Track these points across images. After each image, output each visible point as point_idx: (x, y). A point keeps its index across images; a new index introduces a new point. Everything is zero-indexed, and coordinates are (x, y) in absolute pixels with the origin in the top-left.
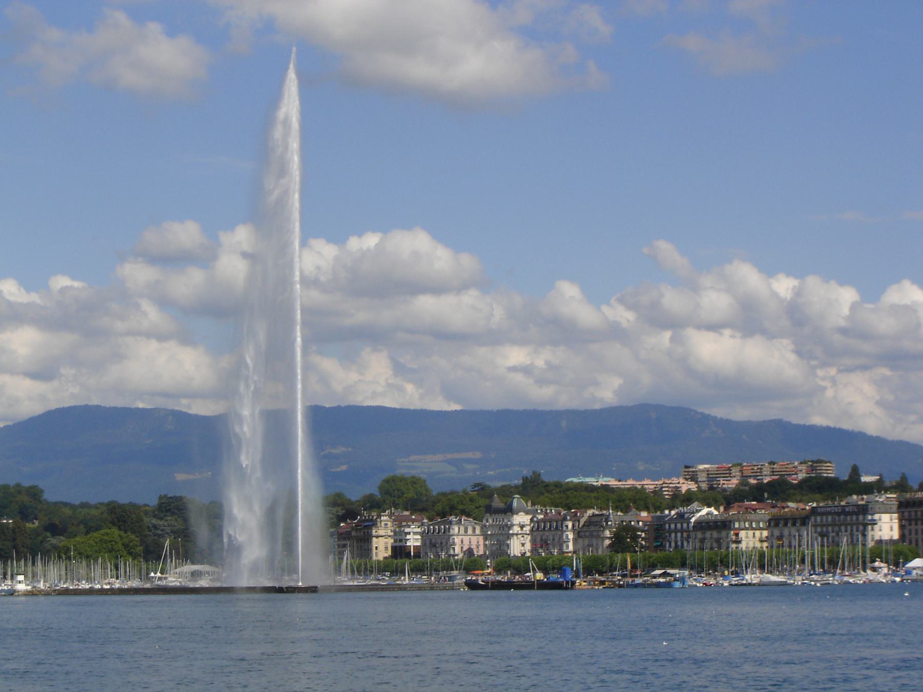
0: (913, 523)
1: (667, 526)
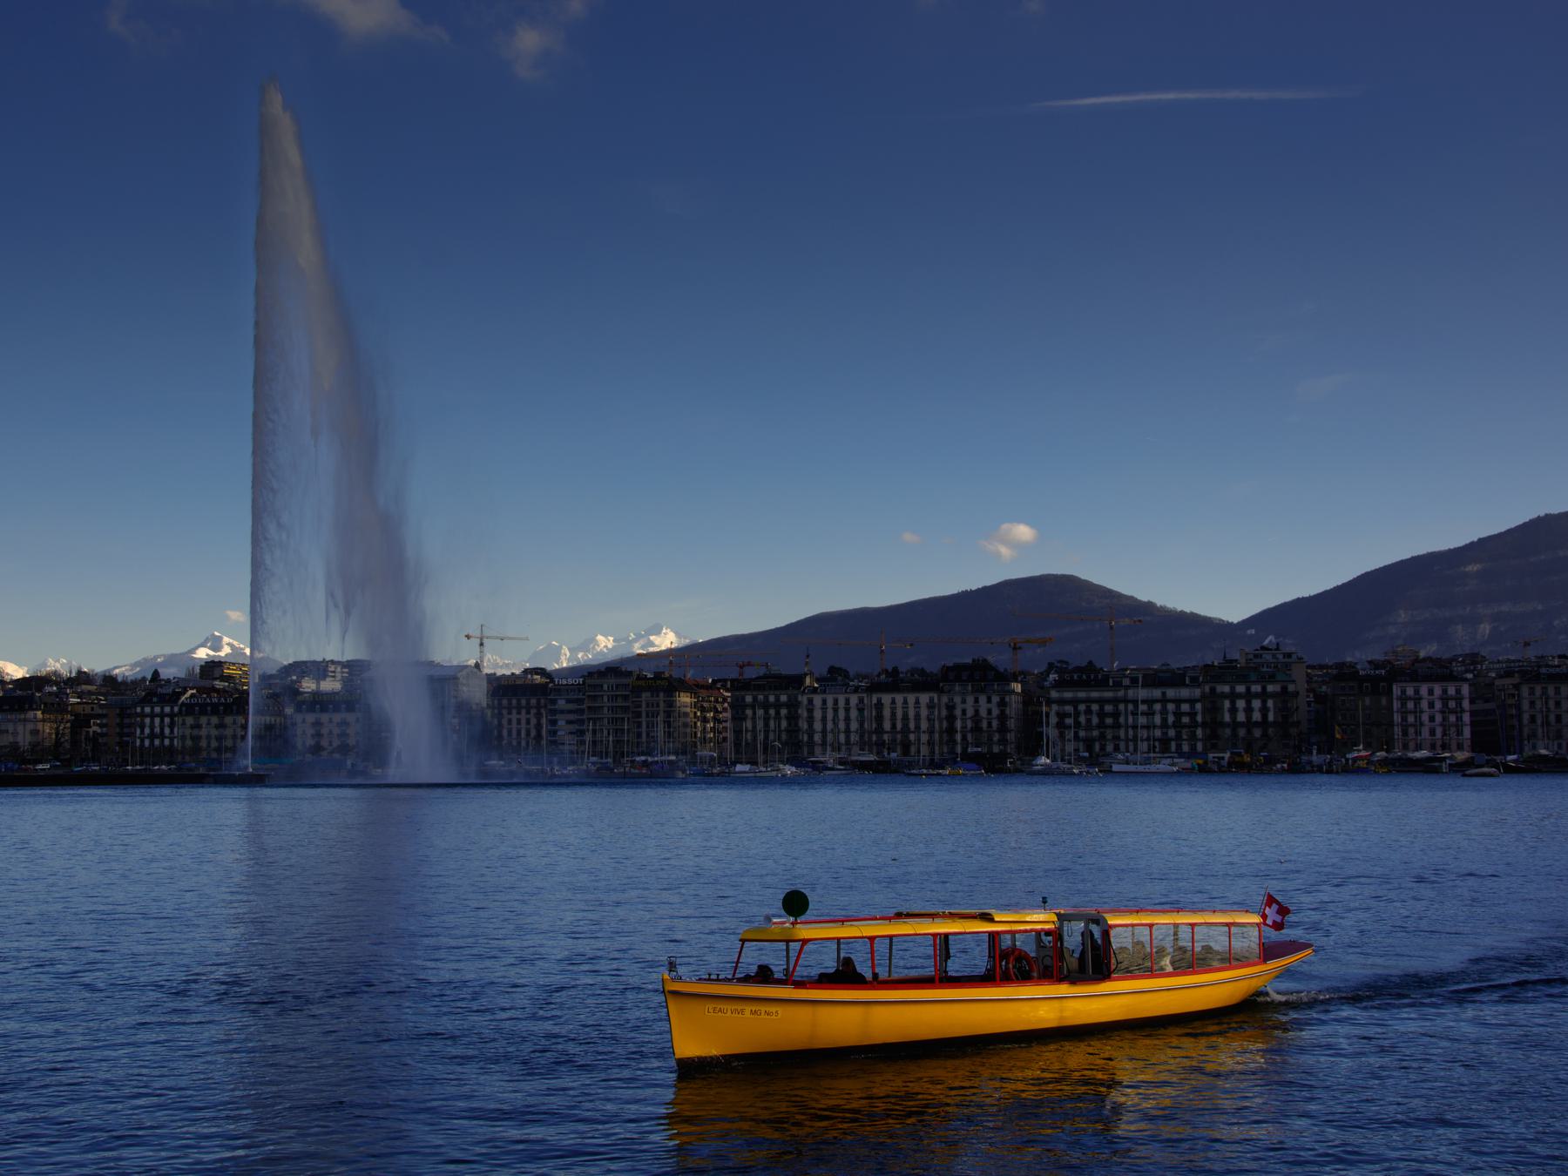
0: (514, 711)
1: (139, 710)
